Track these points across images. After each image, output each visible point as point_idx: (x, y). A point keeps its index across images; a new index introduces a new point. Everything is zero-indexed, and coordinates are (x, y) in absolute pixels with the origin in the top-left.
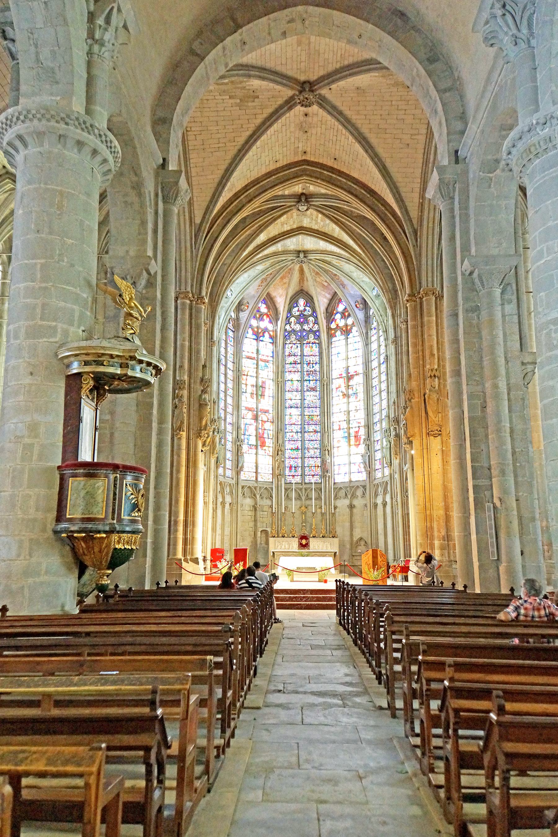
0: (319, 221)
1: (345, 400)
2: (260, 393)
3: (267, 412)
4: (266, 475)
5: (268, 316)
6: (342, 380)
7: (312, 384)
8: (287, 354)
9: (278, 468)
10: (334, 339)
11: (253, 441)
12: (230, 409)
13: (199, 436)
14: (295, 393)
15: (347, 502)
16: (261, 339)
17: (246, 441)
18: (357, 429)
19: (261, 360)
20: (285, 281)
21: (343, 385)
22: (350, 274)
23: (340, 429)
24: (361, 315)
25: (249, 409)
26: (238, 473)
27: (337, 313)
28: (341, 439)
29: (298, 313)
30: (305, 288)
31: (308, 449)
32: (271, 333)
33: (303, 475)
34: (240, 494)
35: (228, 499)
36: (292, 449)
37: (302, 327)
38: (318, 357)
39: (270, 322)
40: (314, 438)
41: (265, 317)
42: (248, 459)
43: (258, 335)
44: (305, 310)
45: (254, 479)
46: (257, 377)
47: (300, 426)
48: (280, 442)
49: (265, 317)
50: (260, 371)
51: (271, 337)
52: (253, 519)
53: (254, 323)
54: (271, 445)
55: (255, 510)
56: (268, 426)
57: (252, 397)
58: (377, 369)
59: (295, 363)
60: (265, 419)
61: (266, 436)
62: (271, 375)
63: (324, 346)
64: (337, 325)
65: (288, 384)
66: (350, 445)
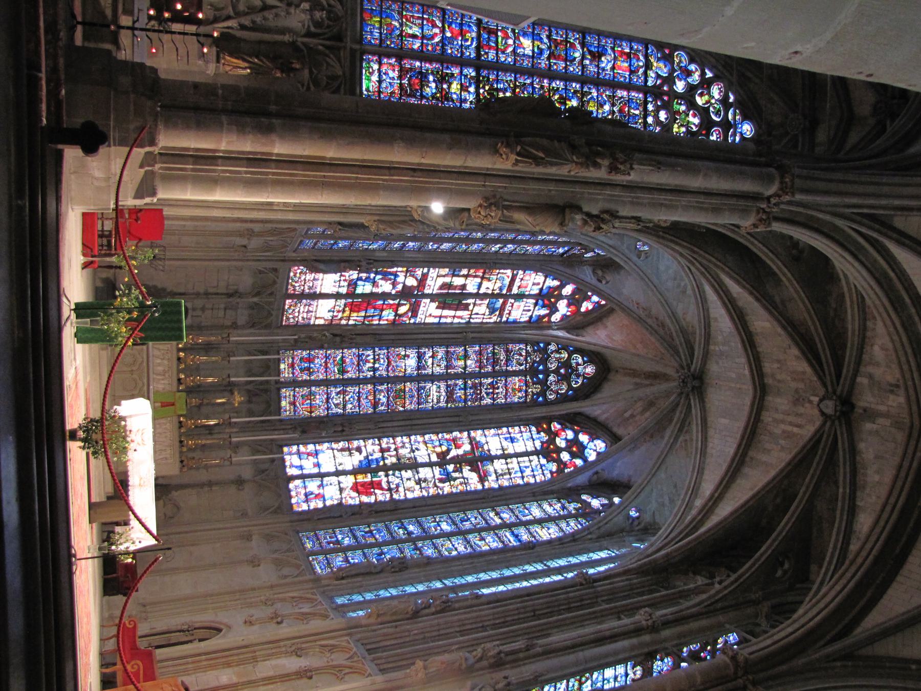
0: (783, 426)
1: (434, 458)
2: (449, 301)
3: (415, 315)
4: (298, 313)
5: (573, 313)
6: (467, 447)
7: (460, 393)
8: (510, 346)
9: (310, 338)
10: (534, 429)
11: (364, 288)
12: (431, 246)
13: (492, 201)
14: (443, 364)
15: (247, 473)
16: (540, 302)
17: (364, 275)
18: (385, 485)
19: (504, 304)
20: (639, 346)
21: (460, 452)
22: (663, 467)
23: (382, 451)
24: (582, 479)
25: (422, 282)
26: (303, 262)
27: (576, 434)
28: (364, 454)
29: (573, 362)
30: (611, 376)
31: (344, 392)
32: (546, 319)
33: (294, 384)
34: (261, 266)
35: (255, 243)
36: (343, 360)
37: (553, 372)
38: (503, 401)
39: (564, 317)
40: (363, 401)
41: (573, 308)
42: (328, 282)
43: (547, 298)
44: (578, 376)
45: (291, 291)
46: (477, 296)
47: (384, 373)
48: (359, 339)
49: (573, 308)
50: (487, 302)
51: (540, 318)
52: (211, 290)
53: (568, 290)
54: (351, 322)
55: (230, 295)
56: (389, 315)
57: (444, 286)
58: (499, 521)
59: (495, 362)
60: (402, 310)
61: (371, 312)
62: (476, 320)
63: (524, 414)
64: (557, 434)
65: (460, 350)
66: (354, 472)
